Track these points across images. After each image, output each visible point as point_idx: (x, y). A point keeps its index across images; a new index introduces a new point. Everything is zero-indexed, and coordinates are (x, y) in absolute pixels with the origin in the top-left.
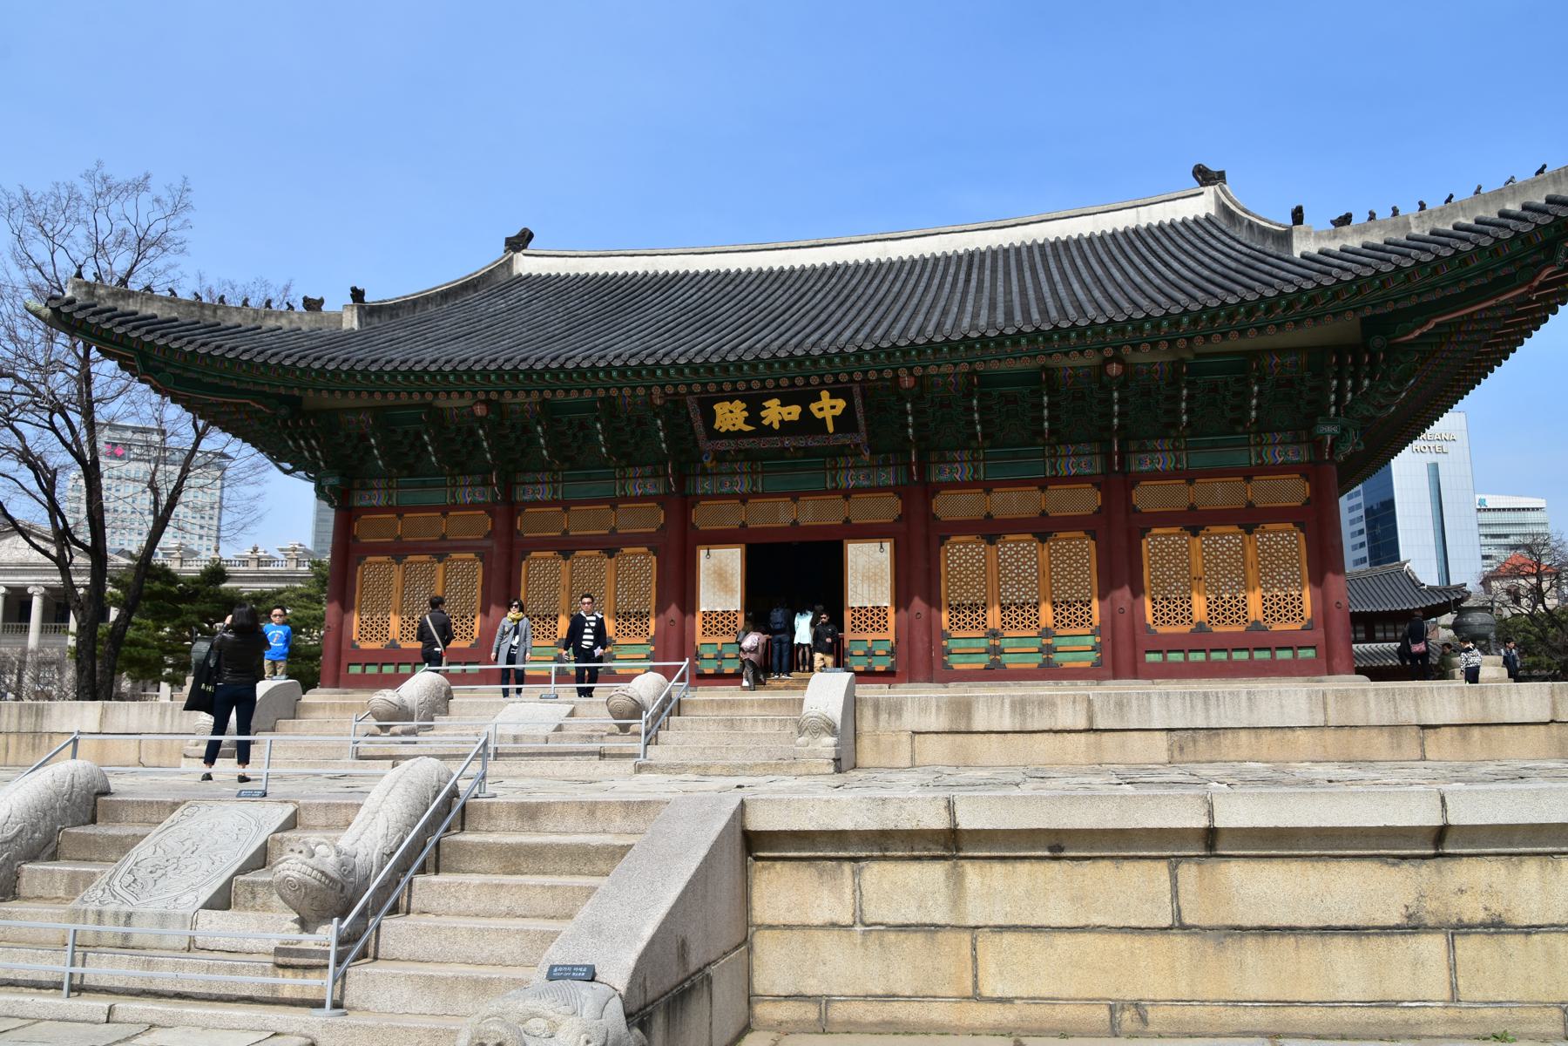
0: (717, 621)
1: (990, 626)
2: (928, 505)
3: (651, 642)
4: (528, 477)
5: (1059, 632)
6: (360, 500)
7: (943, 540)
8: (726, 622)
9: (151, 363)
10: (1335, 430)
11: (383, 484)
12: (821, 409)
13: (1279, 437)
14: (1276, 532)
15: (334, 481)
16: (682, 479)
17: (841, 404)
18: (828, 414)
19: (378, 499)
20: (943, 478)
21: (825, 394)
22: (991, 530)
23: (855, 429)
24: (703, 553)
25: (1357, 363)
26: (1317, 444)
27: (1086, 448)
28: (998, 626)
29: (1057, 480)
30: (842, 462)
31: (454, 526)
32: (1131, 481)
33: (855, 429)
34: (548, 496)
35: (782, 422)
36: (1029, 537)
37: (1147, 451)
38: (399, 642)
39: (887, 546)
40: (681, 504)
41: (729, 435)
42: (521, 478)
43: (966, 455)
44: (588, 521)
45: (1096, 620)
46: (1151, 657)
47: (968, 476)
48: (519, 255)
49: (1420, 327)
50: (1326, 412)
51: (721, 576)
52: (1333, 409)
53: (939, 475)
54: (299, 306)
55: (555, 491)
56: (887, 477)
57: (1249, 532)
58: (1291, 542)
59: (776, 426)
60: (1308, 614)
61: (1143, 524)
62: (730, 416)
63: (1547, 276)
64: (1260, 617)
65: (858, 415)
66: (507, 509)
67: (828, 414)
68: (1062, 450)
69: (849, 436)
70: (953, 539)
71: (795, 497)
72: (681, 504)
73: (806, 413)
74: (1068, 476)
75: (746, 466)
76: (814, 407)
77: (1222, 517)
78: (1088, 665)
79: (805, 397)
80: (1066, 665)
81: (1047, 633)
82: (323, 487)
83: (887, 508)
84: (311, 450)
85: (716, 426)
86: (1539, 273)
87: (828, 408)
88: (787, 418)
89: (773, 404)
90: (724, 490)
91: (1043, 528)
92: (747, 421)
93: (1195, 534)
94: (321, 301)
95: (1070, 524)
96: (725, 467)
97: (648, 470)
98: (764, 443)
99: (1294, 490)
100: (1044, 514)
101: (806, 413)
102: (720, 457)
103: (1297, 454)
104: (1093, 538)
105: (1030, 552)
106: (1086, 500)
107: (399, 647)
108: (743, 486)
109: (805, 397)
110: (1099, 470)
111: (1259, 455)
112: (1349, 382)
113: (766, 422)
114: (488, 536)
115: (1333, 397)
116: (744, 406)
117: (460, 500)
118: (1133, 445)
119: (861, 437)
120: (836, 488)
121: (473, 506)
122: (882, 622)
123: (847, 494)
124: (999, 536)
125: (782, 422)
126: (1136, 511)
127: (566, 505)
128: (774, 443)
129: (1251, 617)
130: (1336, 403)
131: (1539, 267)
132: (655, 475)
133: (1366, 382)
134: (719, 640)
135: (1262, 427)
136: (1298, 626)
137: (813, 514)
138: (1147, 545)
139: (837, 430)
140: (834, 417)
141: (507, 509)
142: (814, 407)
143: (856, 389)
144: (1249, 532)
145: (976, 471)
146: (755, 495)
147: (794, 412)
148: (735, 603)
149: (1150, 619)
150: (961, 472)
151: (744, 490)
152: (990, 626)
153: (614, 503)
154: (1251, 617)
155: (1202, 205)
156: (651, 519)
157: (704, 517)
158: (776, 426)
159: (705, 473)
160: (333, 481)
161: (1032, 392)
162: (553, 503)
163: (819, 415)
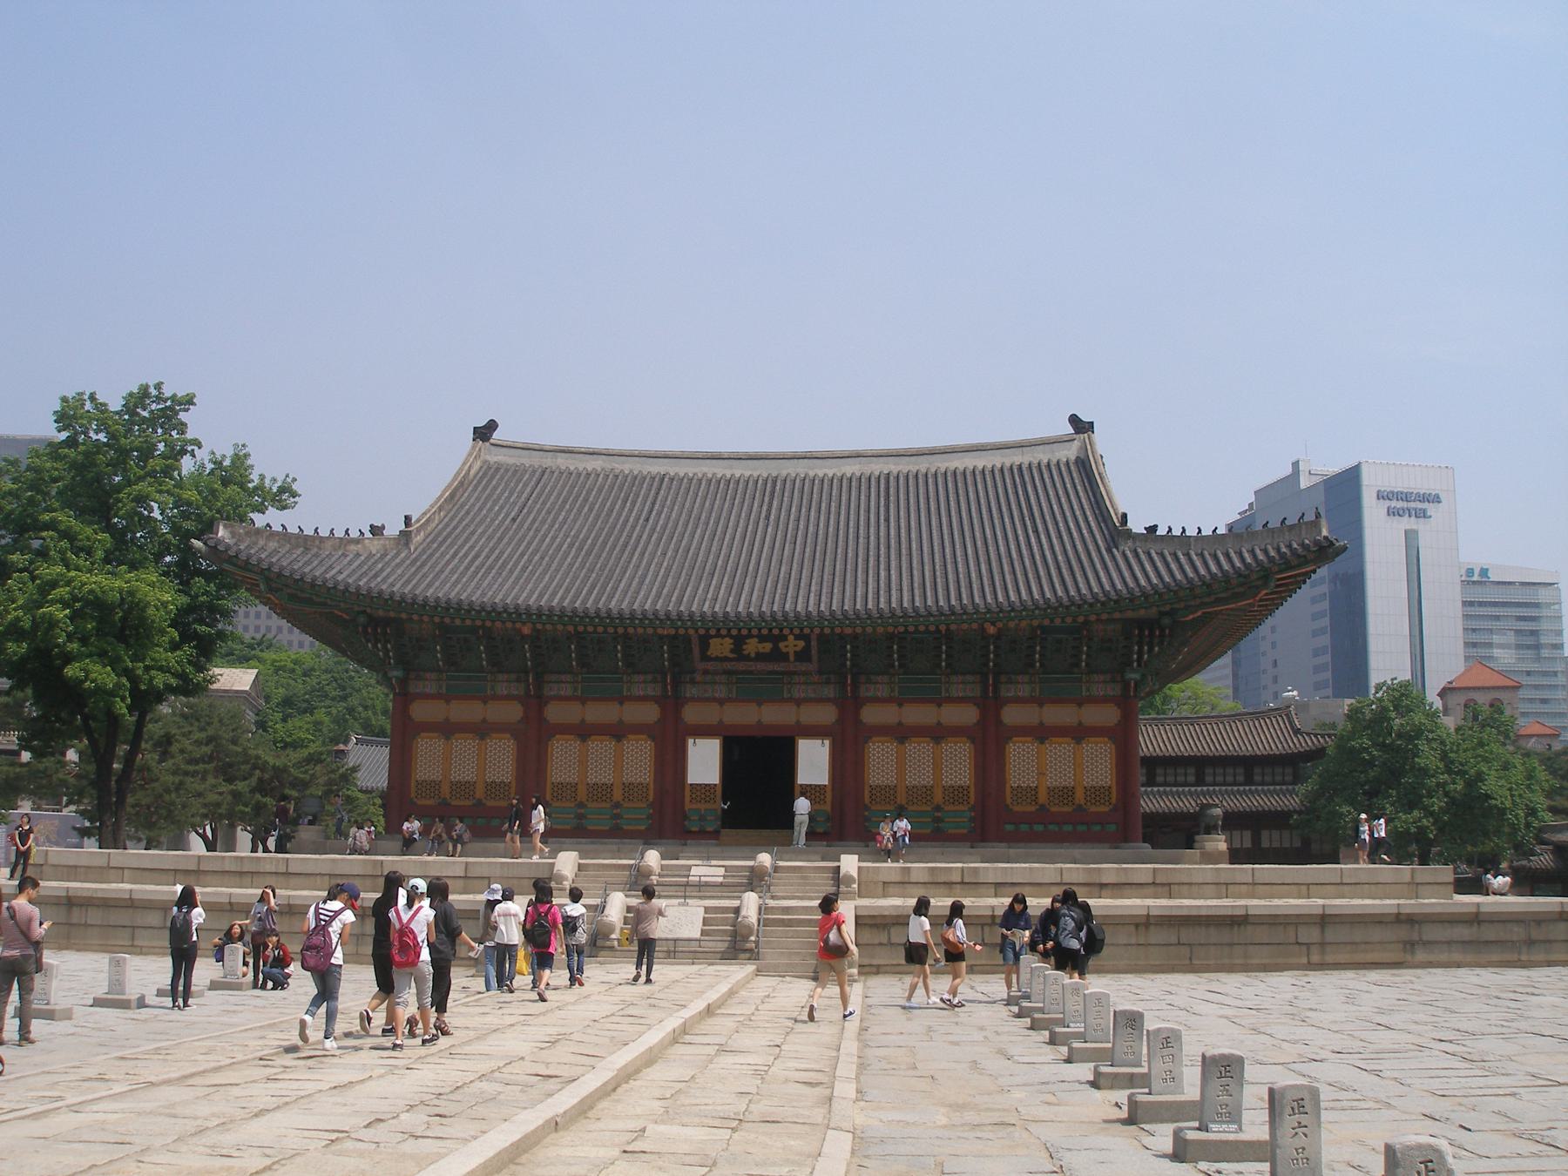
1: (899, 802)
4: (554, 677)
5: (946, 808)
6: (415, 687)
8: (708, 794)
9: (274, 585)
10: (1136, 676)
11: (434, 676)
12: (786, 646)
13: (1102, 678)
14: (1096, 743)
15: (396, 673)
16: (677, 683)
17: (801, 644)
18: (791, 651)
19: (431, 688)
20: (870, 694)
21: (791, 637)
22: (901, 734)
23: (809, 660)
24: (691, 741)
25: (1151, 634)
26: (1126, 685)
27: (970, 678)
28: (904, 802)
30: (796, 679)
32: (999, 703)
33: (809, 660)
34: (570, 693)
35: (758, 654)
36: (928, 739)
37: (1011, 683)
38: (449, 801)
39: (827, 742)
40: (672, 704)
41: (717, 659)
43: (886, 678)
45: (972, 801)
46: (1009, 827)
49: (1193, 613)
50: (1130, 664)
52: (1135, 664)
53: (866, 691)
55: (575, 690)
56: (829, 691)
57: (1078, 742)
58: (1106, 751)
59: (753, 655)
60: (1114, 800)
62: (721, 647)
63: (1266, 594)
64: (1083, 802)
65: (813, 652)
66: (535, 702)
67: (791, 651)
68: (954, 678)
69: (805, 664)
70: (874, 739)
71: (760, 704)
72: (672, 704)
73: (776, 649)
74: (958, 697)
75: (724, 678)
76: (781, 645)
78: (965, 831)
80: (950, 831)
81: (938, 808)
82: (391, 679)
83: (826, 714)
84: (385, 647)
85: (709, 653)
86: (1259, 592)
87: (792, 645)
88: (761, 651)
90: (707, 695)
91: (937, 734)
92: (732, 651)
93: (1042, 743)
94: (383, 527)
95: (957, 732)
96: (709, 677)
98: (741, 666)
99: (1108, 715)
100: (939, 723)
101: (776, 649)
102: (706, 672)
103: (1114, 690)
104: (973, 742)
105: (928, 750)
106: (967, 715)
107: (449, 804)
108: (721, 692)
110: (979, 695)
111: (1088, 690)
112: (1146, 648)
113: (745, 652)
114: (519, 722)
115: (1135, 656)
116: (732, 641)
118: (1003, 678)
119: (812, 667)
120: (791, 698)
121: (508, 698)
122: (822, 797)
123: (799, 702)
124: (907, 738)
125: (758, 654)
126: (1001, 722)
129: (1077, 802)
130: (1139, 660)
132: (654, 681)
133: (1156, 649)
134: (703, 806)
136: (1106, 809)
137: (773, 715)
139: (796, 660)
140: (795, 652)
141: (535, 702)
142: (781, 645)
143: (814, 637)
144: (1078, 742)
145: (892, 691)
146: (729, 700)
147: (768, 646)
149: (1009, 801)
150: (883, 691)
151: (722, 696)
152: (899, 802)
153: (622, 700)
154: (1077, 802)
156: (649, 713)
157: (691, 714)
158: (753, 655)
159: (693, 682)
160: (396, 673)
161: (935, 638)
163: (784, 650)
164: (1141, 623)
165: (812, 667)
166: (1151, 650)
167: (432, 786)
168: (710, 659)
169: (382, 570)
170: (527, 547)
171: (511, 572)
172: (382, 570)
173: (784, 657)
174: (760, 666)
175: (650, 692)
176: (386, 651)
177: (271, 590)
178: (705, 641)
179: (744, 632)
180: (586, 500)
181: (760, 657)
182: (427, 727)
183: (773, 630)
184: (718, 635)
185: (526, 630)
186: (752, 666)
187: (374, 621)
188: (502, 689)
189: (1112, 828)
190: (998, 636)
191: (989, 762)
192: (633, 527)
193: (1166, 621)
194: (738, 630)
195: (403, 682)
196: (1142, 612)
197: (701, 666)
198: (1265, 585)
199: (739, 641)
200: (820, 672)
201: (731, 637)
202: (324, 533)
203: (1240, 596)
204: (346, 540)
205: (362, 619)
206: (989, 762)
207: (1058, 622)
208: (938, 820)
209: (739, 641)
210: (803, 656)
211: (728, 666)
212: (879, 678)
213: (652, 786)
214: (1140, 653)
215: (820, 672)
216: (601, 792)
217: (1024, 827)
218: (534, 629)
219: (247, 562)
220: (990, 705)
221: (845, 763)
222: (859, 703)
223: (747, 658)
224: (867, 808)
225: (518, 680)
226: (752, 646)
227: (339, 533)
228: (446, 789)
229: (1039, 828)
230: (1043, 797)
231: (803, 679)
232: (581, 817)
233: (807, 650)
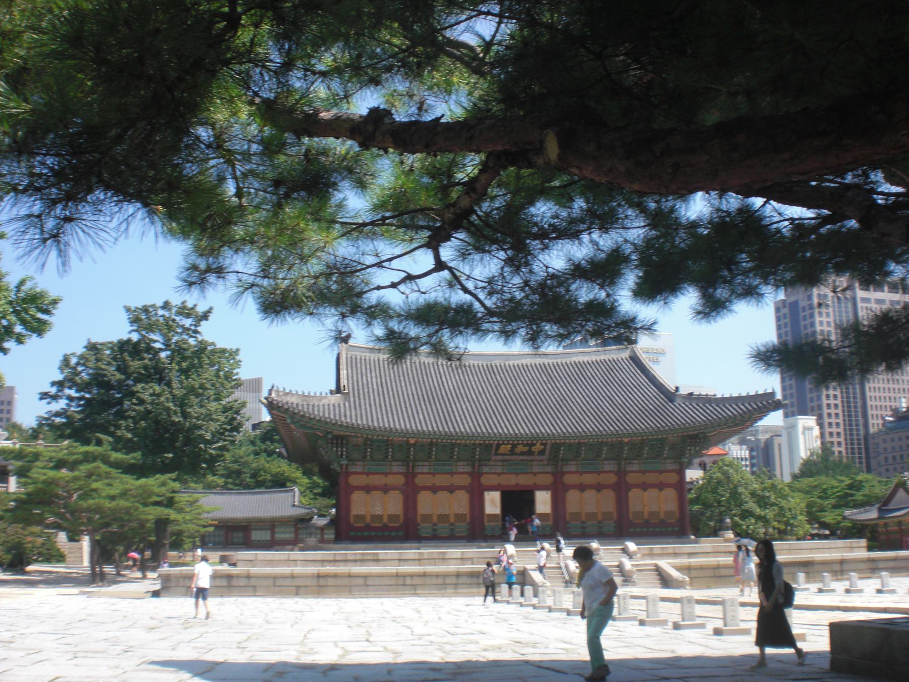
0: (492, 517)
4: (420, 463)
17: (542, 447)
19: (359, 469)
20: (567, 470)
24: (486, 493)
27: (612, 462)
30: (534, 463)
31: (391, 480)
39: (549, 492)
40: (476, 476)
42: (417, 463)
44: (442, 480)
46: (632, 530)
51: (493, 502)
54: (329, 395)
55: (430, 469)
56: (549, 469)
61: (629, 487)
71: (517, 474)
72: (476, 476)
75: (500, 463)
76: (533, 448)
77: (652, 486)
81: (600, 522)
84: (342, 451)
87: (538, 447)
92: (510, 451)
97: (465, 463)
103: (675, 467)
117: (393, 471)
119: (546, 457)
123: (535, 474)
127: (434, 474)
134: (493, 524)
135: (666, 458)
137: (523, 481)
138: (631, 494)
141: (410, 476)
146: (503, 473)
147: (526, 449)
148: (497, 510)
150: (573, 468)
157: (485, 480)
160: (344, 462)
164: (690, 437)
165: (546, 457)
174: (521, 457)
176: (342, 451)
177: (293, 423)
178: (498, 446)
179: (516, 442)
181: (522, 453)
191: (622, 503)
193: (701, 436)
196: (691, 433)
197: (493, 458)
199: (514, 446)
202: (312, 394)
204: (321, 398)
205: (330, 436)
206: (622, 503)
209: (514, 446)
210: (542, 453)
211: (506, 457)
212: (572, 462)
213: (468, 515)
214: (690, 450)
216: (443, 518)
219: (287, 410)
221: (558, 502)
227: (318, 395)
229: (645, 530)
230: (646, 516)
231: (537, 463)
232: (435, 530)
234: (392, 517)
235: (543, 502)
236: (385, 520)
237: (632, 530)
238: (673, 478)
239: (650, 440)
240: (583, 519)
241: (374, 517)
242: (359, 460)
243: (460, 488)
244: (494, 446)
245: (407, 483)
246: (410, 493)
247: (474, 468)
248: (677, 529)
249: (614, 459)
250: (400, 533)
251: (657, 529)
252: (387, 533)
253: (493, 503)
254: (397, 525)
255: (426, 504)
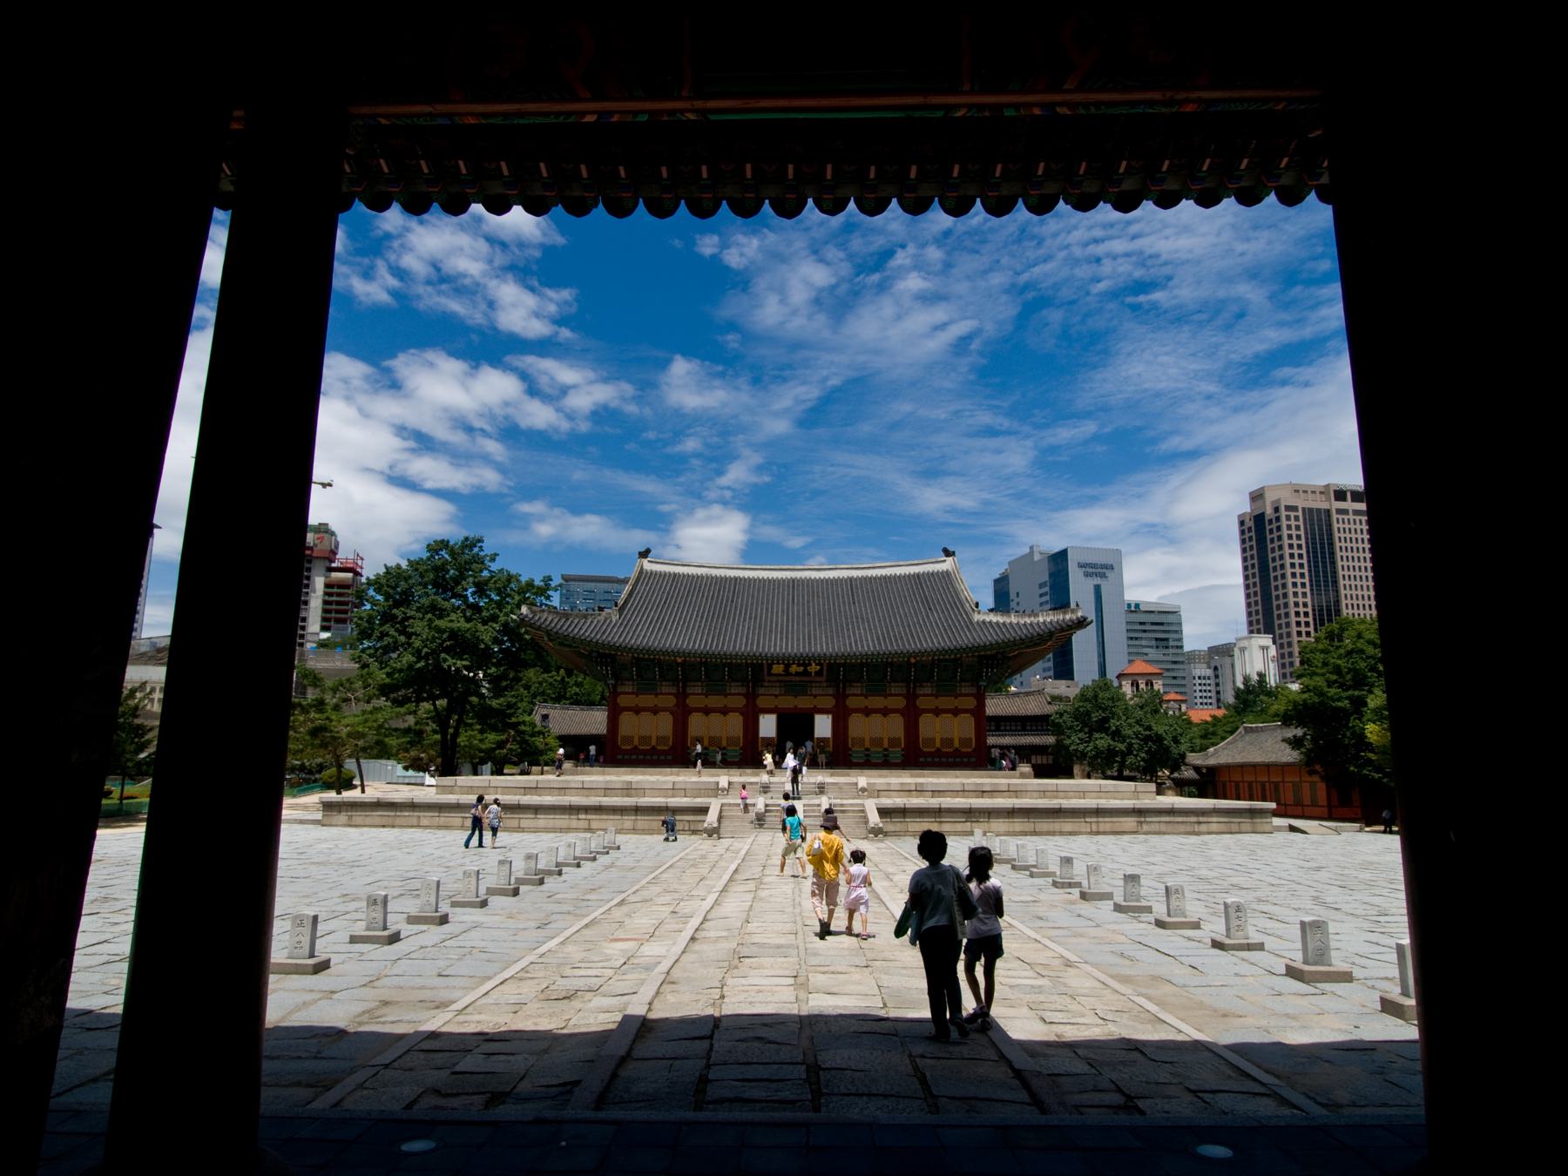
2: (844, 702)
3: (741, 749)
7: (849, 715)
15: (613, 682)
17: (818, 667)
20: (851, 692)
24: (761, 717)
26: (979, 688)
29: (891, 695)
39: (830, 716)
40: (751, 697)
41: (776, 675)
42: (689, 684)
47: (859, 692)
48: (645, 562)
56: (830, 691)
66: (682, 696)
72: (751, 697)
73: (805, 670)
79: (805, 665)
81: (886, 750)
83: (829, 702)
84: (607, 671)
87: (814, 668)
89: (794, 666)
98: (788, 678)
101: (805, 670)
102: (769, 681)
103: (974, 690)
109: (805, 665)
119: (824, 679)
123: (815, 696)
128: (793, 678)
131: (1047, 641)
137: (803, 702)
141: (682, 696)
146: (780, 695)
147: (801, 669)
155: (947, 565)
156: (740, 702)
157: (762, 702)
159: (762, 686)
160: (613, 682)
162: (702, 694)
166: (992, 671)
167: (629, 739)
168: (772, 675)
169: (606, 630)
170: (676, 616)
171: (670, 630)
172: (606, 630)
173: (809, 674)
174: (797, 679)
175: (741, 691)
176: (607, 671)
177: (551, 640)
178: (770, 666)
180: (699, 591)
181: (797, 674)
182: (628, 709)
183: (804, 661)
184: (778, 663)
185: (679, 660)
186: (793, 678)
187: (601, 655)
188: (664, 690)
189: (973, 760)
190: (915, 664)
191: (912, 728)
192: (726, 605)
194: (787, 661)
195: (615, 686)
198: (1050, 639)
199: (787, 666)
200: (827, 681)
201: (783, 663)
203: (1036, 645)
205: (595, 654)
206: (912, 728)
207: (947, 657)
208: (885, 756)
209: (787, 666)
210: (819, 673)
211: (781, 678)
215: (827, 681)
217: (929, 760)
218: (685, 661)
220: (911, 698)
221: (839, 727)
222: (846, 696)
223: (791, 674)
224: (850, 749)
225: (673, 685)
226: (794, 669)
228: (636, 742)
229: (937, 760)
233: (821, 670)
234: (660, 739)
235: (823, 726)
236: (654, 742)
237: (921, 759)
238: (971, 703)
239: (939, 660)
240: (867, 744)
241: (644, 739)
242: (629, 680)
243: (734, 710)
244: (765, 666)
245: (677, 705)
246: (681, 716)
247: (748, 690)
248: (973, 760)
249: (901, 682)
250: (669, 757)
251: (951, 760)
252: (655, 757)
253: (768, 726)
254: (666, 748)
255: (698, 725)
